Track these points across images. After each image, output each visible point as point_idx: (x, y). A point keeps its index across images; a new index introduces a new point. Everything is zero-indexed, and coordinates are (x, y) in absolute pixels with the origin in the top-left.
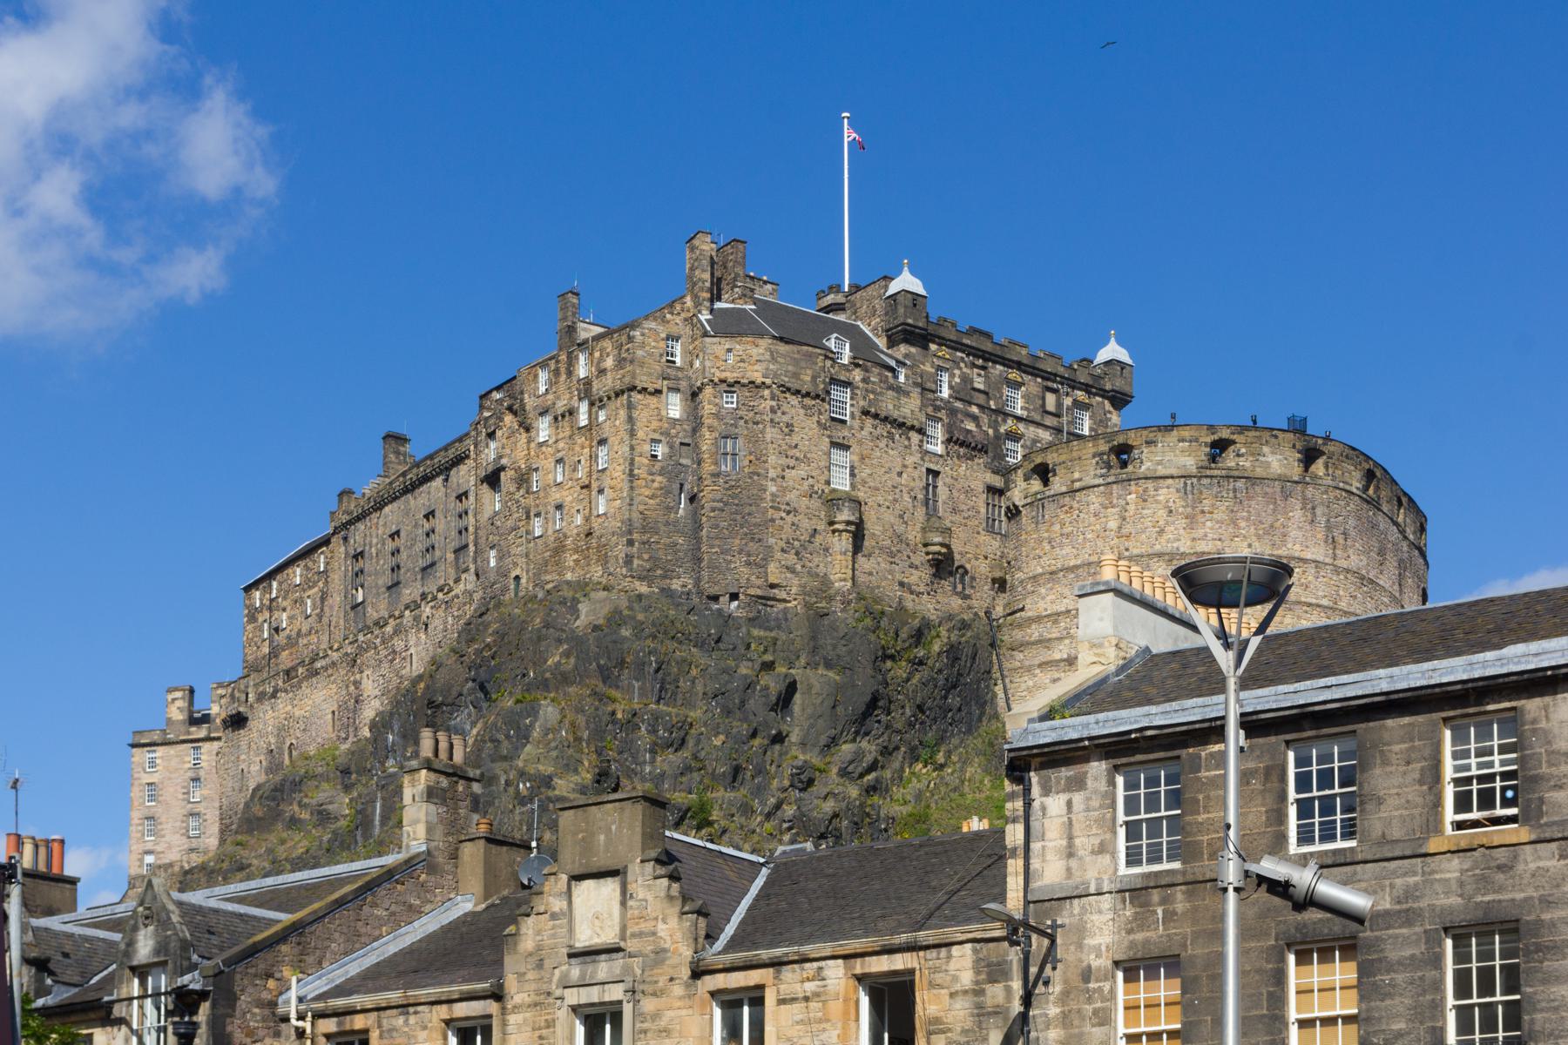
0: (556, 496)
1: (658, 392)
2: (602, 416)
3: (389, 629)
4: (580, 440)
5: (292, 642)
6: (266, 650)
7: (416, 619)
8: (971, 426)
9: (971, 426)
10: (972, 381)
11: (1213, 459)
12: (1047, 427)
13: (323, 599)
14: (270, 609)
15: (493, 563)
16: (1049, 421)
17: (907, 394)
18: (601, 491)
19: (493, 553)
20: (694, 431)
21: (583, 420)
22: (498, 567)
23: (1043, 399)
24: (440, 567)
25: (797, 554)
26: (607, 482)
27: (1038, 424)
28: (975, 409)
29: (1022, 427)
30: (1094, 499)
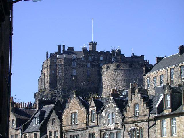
1: (53, 65)
8: (94, 63)
9: (94, 63)
10: (95, 57)
11: (117, 67)
12: (107, 61)
16: (107, 60)
17: (84, 61)
23: (107, 58)
25: (68, 84)
27: (105, 61)
28: (95, 61)
29: (103, 62)
30: (105, 72)
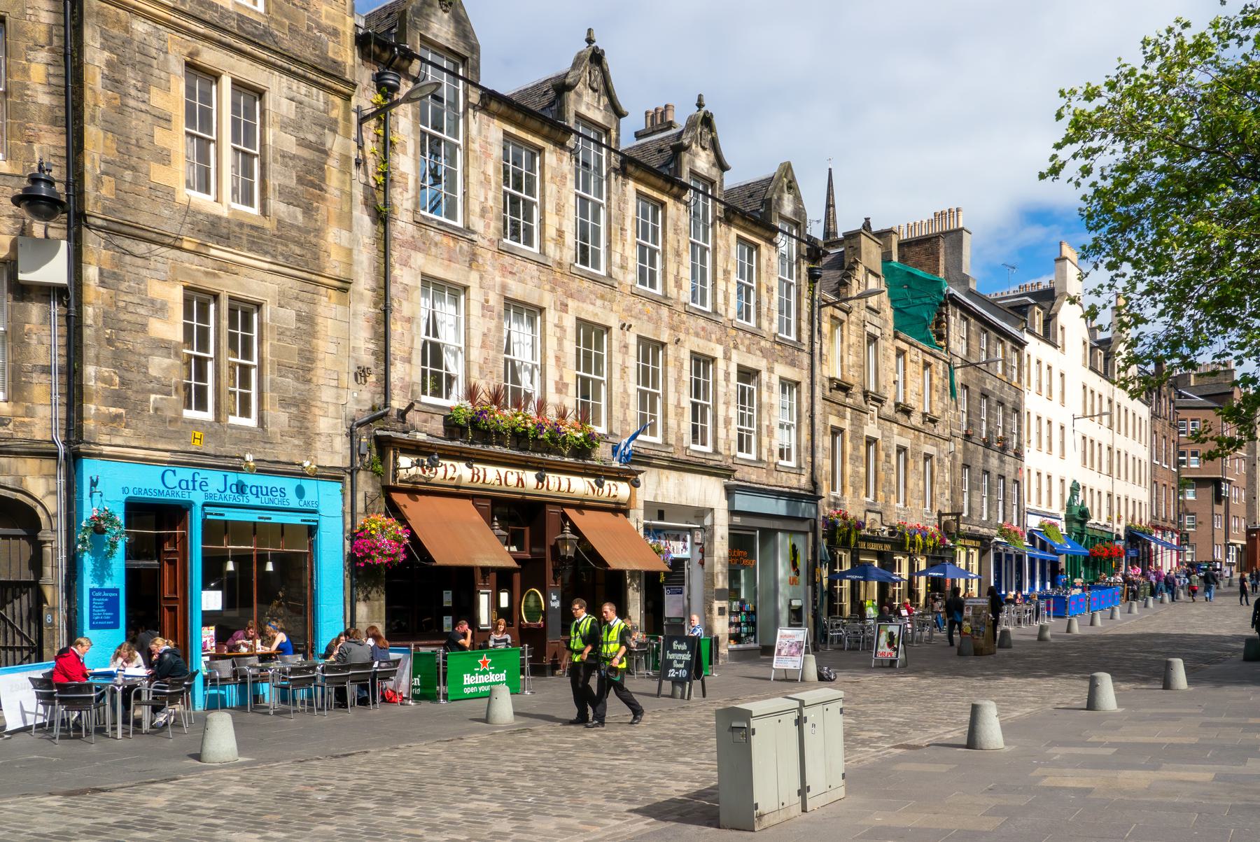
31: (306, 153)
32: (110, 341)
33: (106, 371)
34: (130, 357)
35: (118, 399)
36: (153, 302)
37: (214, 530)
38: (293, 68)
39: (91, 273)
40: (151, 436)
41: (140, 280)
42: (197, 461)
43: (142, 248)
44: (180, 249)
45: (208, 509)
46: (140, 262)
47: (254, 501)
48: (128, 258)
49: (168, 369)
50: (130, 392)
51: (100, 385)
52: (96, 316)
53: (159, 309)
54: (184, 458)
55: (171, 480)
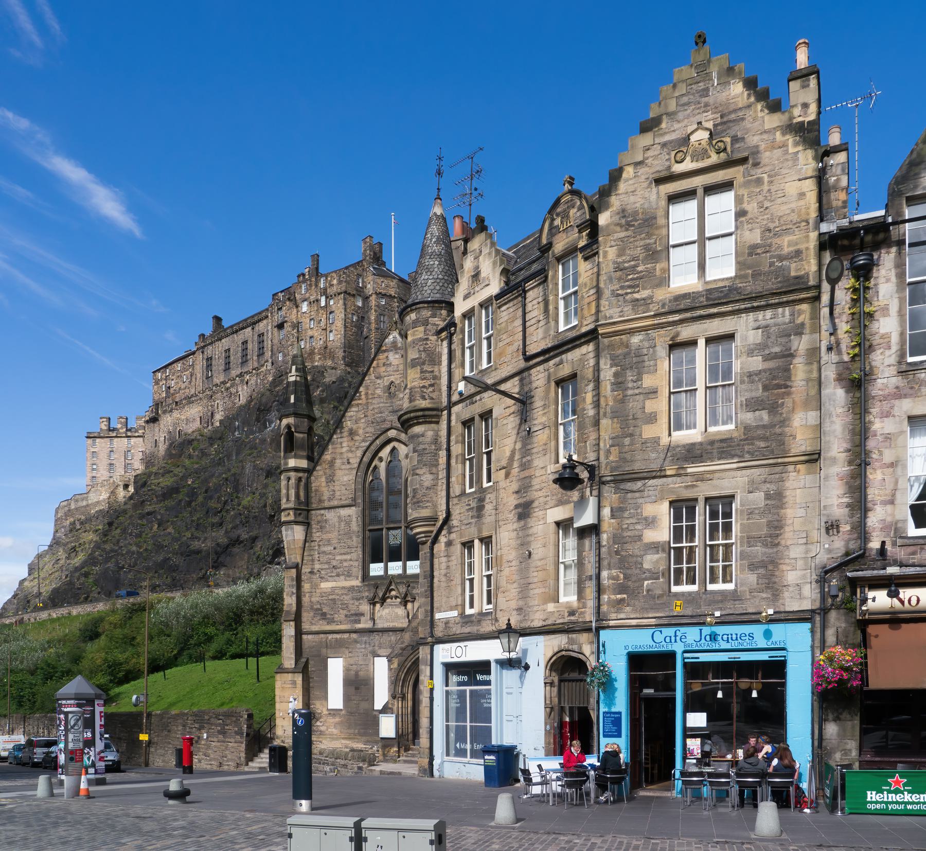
0: (310, 333)
2: (332, 302)
3: (228, 385)
4: (321, 312)
5: (176, 392)
6: (164, 395)
7: (242, 381)
13: (191, 376)
14: (166, 380)
15: (280, 359)
18: (331, 331)
19: (281, 355)
20: (367, 312)
21: (323, 304)
22: (283, 361)
24: (250, 363)
26: (334, 328)
31: (771, 364)
32: (617, 553)
33: (614, 572)
34: (631, 560)
35: (622, 589)
36: (646, 519)
37: (694, 670)
38: (755, 304)
39: (606, 512)
40: (644, 609)
41: (638, 507)
42: (676, 622)
43: (639, 484)
44: (665, 476)
45: (686, 655)
46: (637, 495)
47: (724, 645)
48: (629, 495)
49: (657, 561)
50: (630, 583)
51: (611, 581)
52: (608, 539)
53: (651, 522)
54: (665, 621)
55: (659, 637)
